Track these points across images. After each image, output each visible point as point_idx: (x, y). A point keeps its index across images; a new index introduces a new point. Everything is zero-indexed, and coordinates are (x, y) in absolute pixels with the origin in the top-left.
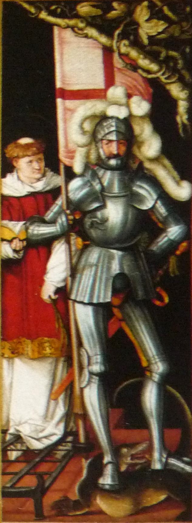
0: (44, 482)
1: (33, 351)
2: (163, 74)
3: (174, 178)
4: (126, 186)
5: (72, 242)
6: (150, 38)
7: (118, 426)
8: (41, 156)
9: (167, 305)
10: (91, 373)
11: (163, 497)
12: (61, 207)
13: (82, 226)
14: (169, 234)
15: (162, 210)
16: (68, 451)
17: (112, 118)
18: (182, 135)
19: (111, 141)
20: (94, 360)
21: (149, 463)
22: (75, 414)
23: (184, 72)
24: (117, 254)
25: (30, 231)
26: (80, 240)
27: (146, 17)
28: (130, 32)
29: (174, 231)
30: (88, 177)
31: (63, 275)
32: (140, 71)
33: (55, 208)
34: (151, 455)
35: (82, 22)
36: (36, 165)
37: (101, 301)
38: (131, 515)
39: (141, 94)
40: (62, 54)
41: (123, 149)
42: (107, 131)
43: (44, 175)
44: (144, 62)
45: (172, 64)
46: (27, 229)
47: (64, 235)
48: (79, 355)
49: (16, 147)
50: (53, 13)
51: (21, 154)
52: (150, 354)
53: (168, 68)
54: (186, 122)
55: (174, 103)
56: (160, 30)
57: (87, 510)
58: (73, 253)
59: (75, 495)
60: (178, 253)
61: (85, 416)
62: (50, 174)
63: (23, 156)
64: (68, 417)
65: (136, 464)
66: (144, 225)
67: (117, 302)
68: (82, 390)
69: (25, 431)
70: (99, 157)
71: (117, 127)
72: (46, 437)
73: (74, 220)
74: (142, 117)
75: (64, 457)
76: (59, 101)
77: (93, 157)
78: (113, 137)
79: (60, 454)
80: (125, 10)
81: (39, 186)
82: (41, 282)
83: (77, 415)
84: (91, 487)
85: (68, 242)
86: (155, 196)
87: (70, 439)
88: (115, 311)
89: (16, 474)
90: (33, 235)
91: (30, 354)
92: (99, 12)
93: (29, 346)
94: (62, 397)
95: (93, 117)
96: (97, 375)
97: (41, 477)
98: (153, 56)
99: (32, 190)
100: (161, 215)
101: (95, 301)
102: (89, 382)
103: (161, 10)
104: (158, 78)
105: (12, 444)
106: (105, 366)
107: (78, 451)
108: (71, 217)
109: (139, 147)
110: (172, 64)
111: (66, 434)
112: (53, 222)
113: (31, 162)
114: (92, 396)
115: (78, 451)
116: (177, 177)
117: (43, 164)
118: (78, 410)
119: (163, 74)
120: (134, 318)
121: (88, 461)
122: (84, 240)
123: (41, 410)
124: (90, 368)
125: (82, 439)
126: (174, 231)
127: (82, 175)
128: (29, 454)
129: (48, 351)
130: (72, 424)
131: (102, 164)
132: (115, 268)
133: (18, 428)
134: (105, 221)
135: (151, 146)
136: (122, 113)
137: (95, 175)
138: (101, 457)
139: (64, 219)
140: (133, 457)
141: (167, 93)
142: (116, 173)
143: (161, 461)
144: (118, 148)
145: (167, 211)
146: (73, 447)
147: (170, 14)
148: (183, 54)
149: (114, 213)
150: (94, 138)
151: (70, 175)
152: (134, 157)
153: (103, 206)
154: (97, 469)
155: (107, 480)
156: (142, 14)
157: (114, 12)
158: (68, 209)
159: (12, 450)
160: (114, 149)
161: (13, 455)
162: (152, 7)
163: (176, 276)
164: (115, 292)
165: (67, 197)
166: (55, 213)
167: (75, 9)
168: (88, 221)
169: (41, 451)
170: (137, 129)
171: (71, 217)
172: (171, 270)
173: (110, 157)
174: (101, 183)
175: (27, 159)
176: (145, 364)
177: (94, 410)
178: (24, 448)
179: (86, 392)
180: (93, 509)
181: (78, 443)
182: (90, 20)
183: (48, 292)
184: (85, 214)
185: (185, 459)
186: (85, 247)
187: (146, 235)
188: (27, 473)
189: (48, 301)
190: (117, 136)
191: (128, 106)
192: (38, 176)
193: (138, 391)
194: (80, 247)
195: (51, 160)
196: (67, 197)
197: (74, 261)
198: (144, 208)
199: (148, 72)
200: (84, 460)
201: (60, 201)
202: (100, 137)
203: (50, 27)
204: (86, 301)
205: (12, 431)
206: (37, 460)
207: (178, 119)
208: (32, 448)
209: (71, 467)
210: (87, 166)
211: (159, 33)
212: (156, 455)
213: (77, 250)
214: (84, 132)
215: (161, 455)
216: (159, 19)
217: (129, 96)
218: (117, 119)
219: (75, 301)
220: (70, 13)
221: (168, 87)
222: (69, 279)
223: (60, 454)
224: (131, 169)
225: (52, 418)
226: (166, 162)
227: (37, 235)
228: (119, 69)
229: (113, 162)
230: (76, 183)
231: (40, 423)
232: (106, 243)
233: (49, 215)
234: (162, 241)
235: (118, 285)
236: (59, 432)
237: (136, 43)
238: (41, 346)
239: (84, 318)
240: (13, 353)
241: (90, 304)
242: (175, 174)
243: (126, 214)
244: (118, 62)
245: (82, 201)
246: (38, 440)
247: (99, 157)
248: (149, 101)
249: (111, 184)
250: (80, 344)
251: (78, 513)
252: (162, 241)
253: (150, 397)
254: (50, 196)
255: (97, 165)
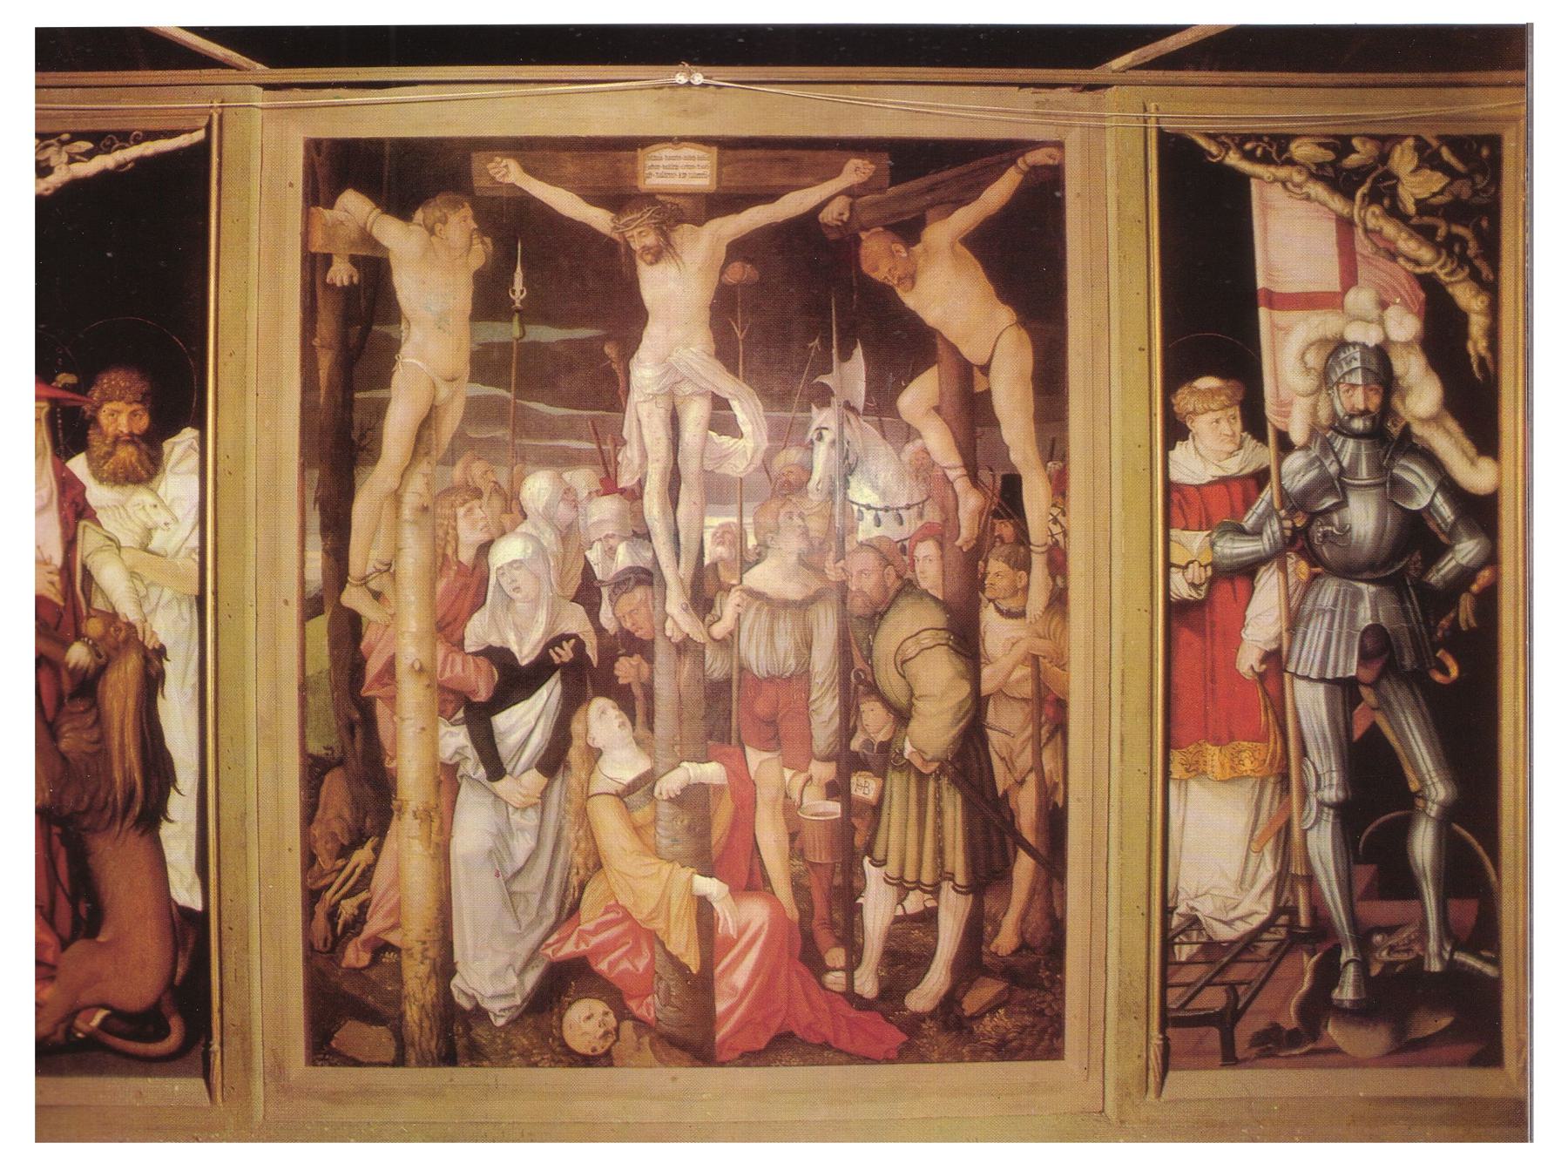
0: (1237, 999)
1: (1222, 765)
2: (1442, 267)
3: (1464, 453)
4: (1381, 469)
5: (1290, 570)
6: (1419, 203)
7: (1368, 895)
8: (1236, 411)
9: (1455, 682)
10: (1321, 804)
11: (1445, 1021)
12: (1271, 503)
13: (1307, 538)
14: (1459, 556)
15: (1446, 511)
16: (1282, 942)
17: (1354, 344)
18: (1478, 376)
19: (1354, 386)
20: (1325, 781)
21: (1419, 960)
22: (1291, 875)
23: (1477, 263)
24: (1368, 590)
25: (1218, 549)
26: (1303, 566)
27: (1411, 167)
28: (1384, 192)
29: (1467, 550)
30: (1315, 451)
31: (1273, 631)
32: (1401, 261)
33: (1260, 507)
34: (1425, 948)
35: (1300, 172)
36: (1225, 427)
37: (1340, 675)
38: (1389, 1054)
39: (1405, 303)
40: (1265, 228)
41: (1375, 401)
42: (1346, 369)
43: (1240, 447)
44: (1408, 245)
45: (1457, 249)
46: (1213, 545)
47: (1276, 556)
48: (1301, 771)
49: (1192, 393)
50: (1249, 156)
51: (1199, 406)
52: (1424, 770)
53: (1450, 254)
54: (1483, 352)
55: (1460, 319)
56: (1435, 189)
57: (1310, 1046)
58: (1291, 589)
59: (1290, 1020)
60: (1475, 588)
61: (1310, 879)
62: (1250, 443)
63: (1206, 411)
64: (1283, 879)
65: (1397, 963)
66: (1415, 538)
67: (1368, 675)
68: (1304, 833)
69: (1205, 908)
70: (1334, 415)
71: (1363, 361)
72: (1241, 918)
73: (1294, 529)
74: (1407, 344)
75: (1273, 952)
76: (1263, 313)
77: (1324, 414)
78: (1357, 378)
79: (1265, 948)
80: (1376, 153)
81: (1233, 467)
82: (1234, 640)
83: (1295, 876)
84: (1318, 1007)
85: (1283, 568)
86: (1433, 487)
87: (1283, 919)
88: (1364, 691)
89: (1188, 985)
90: (1224, 557)
91: (1217, 770)
92: (1329, 156)
93: (1214, 756)
94: (1269, 846)
95: (1323, 342)
96: (1330, 806)
97: (1232, 987)
98: (1425, 234)
99: (1221, 473)
100: (1444, 520)
101: (1329, 675)
102: (1317, 821)
103: (1437, 153)
104: (1433, 273)
105: (1182, 932)
106: (1345, 790)
107: (1296, 940)
108: (1288, 524)
109: (1403, 401)
110: (1457, 249)
111: (1278, 911)
112: (1257, 532)
113: (1217, 421)
114: (1322, 843)
115: (1296, 940)
116: (1472, 451)
117: (1238, 426)
118: (1297, 869)
119: (1442, 267)
120: (1396, 706)
121: (1315, 958)
122: (1312, 564)
123: (1234, 871)
124: (1319, 794)
125: (1304, 920)
126: (1467, 550)
127: (1306, 447)
128: (1211, 947)
129: (1248, 765)
130: (1286, 894)
131: (1340, 427)
132: (1365, 616)
133: (1191, 903)
134: (1345, 530)
135: (1422, 396)
136: (1372, 337)
137: (1327, 446)
138: (1336, 951)
139: (1276, 527)
140: (1392, 949)
141: (1450, 301)
142: (1364, 444)
143: (1440, 955)
144: (1366, 399)
145: (1454, 512)
146: (1289, 932)
147: (1453, 161)
148: (1478, 233)
149: (1362, 517)
150: (1326, 379)
151: (1285, 445)
152: (1396, 414)
153: (1342, 504)
154: (1328, 974)
155: (1346, 992)
156: (1403, 161)
157: (1354, 157)
158: (1283, 506)
159: (1182, 943)
160: (1358, 400)
161: (1183, 952)
162: (1421, 146)
163: (1471, 629)
164: (1365, 658)
165: (1281, 488)
166: (1260, 517)
167: (1286, 149)
168: (1318, 531)
169: (1232, 943)
170: (1398, 367)
171: (1288, 524)
172: (1462, 616)
173: (1352, 417)
174: (1340, 463)
175: (1210, 416)
176: (1414, 786)
177: (1326, 872)
178: (1204, 940)
179: (1312, 836)
180: (1321, 1045)
181: (1297, 929)
182: (1313, 168)
183: (1248, 660)
184: (1313, 517)
185: (1485, 953)
186: (1314, 577)
187: (1417, 556)
188: (1209, 983)
189: (1249, 675)
190: (1364, 377)
191: (1381, 322)
192: (1230, 447)
193: (1401, 832)
194: (1304, 578)
195: (1254, 421)
196: (1281, 488)
197: (1293, 603)
198: (1414, 507)
199: (1417, 263)
200: (1305, 958)
201: (1269, 494)
202: (1334, 379)
203: (1243, 180)
204: (1314, 676)
205: (1182, 909)
206: (1225, 959)
207: (1470, 346)
208: (1216, 939)
209: (1285, 969)
210: (1313, 432)
211: (1434, 195)
212: (1433, 946)
213: (1298, 582)
214: (1308, 370)
215: (1441, 947)
216: (1433, 168)
217: (1383, 305)
218: (1364, 346)
219: (1294, 675)
220: (1279, 156)
221: (1450, 290)
222: (1285, 636)
223: (1265, 948)
224: (1388, 438)
225: (1252, 886)
226: (1452, 425)
227: (1232, 557)
228: (1364, 256)
229: (1358, 424)
230: (1295, 461)
231: (1231, 893)
232: (1348, 571)
233: (1249, 521)
234: (1447, 566)
235: (1369, 644)
236: (1264, 910)
237: (1395, 212)
238: (1235, 760)
239: (1310, 704)
240: (1187, 770)
241: (1322, 680)
242: (1467, 444)
243: (1381, 518)
244: (1362, 245)
245: (1307, 492)
246: (1229, 923)
247: (1334, 415)
248: (1418, 314)
249: (1355, 460)
250: (1304, 752)
251: (1296, 1052)
252: (1447, 566)
253: (1423, 844)
254: (1251, 483)
255: (1331, 427)
